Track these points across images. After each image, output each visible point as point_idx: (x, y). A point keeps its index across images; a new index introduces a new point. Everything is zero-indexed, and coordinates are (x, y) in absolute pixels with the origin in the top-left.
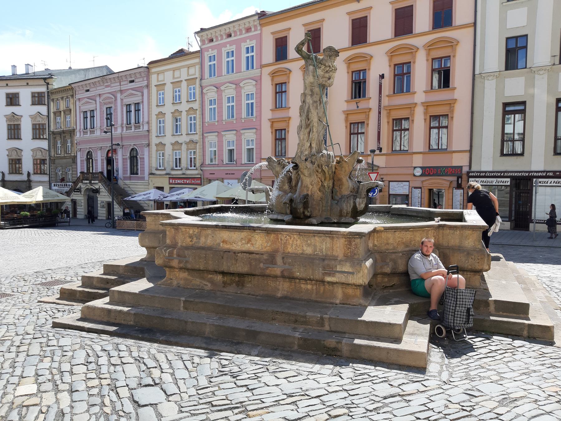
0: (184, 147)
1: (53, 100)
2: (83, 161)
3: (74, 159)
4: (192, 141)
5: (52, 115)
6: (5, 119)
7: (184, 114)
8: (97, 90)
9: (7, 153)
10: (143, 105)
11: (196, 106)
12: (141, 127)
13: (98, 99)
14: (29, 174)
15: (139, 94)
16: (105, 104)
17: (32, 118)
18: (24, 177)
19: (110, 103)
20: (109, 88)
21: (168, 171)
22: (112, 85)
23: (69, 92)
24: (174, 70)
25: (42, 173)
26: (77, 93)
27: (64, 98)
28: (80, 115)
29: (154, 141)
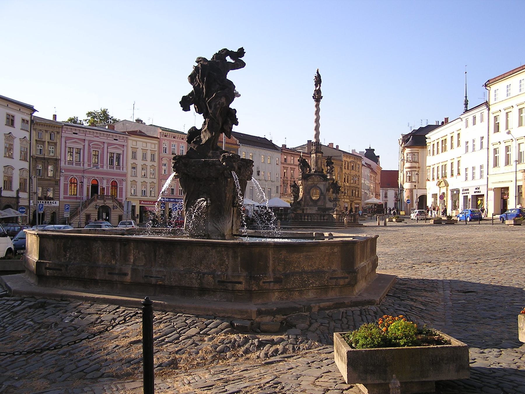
1: (35, 129)
2: (68, 184)
3: (57, 183)
5: (33, 142)
6: (4, 137)
7: (149, 167)
8: (85, 136)
10: (123, 156)
11: (156, 164)
14: (18, 192)
15: (123, 149)
18: (13, 194)
19: (97, 148)
22: (101, 137)
23: (55, 128)
25: (25, 191)
26: (63, 132)
27: (49, 132)
29: (130, 179)
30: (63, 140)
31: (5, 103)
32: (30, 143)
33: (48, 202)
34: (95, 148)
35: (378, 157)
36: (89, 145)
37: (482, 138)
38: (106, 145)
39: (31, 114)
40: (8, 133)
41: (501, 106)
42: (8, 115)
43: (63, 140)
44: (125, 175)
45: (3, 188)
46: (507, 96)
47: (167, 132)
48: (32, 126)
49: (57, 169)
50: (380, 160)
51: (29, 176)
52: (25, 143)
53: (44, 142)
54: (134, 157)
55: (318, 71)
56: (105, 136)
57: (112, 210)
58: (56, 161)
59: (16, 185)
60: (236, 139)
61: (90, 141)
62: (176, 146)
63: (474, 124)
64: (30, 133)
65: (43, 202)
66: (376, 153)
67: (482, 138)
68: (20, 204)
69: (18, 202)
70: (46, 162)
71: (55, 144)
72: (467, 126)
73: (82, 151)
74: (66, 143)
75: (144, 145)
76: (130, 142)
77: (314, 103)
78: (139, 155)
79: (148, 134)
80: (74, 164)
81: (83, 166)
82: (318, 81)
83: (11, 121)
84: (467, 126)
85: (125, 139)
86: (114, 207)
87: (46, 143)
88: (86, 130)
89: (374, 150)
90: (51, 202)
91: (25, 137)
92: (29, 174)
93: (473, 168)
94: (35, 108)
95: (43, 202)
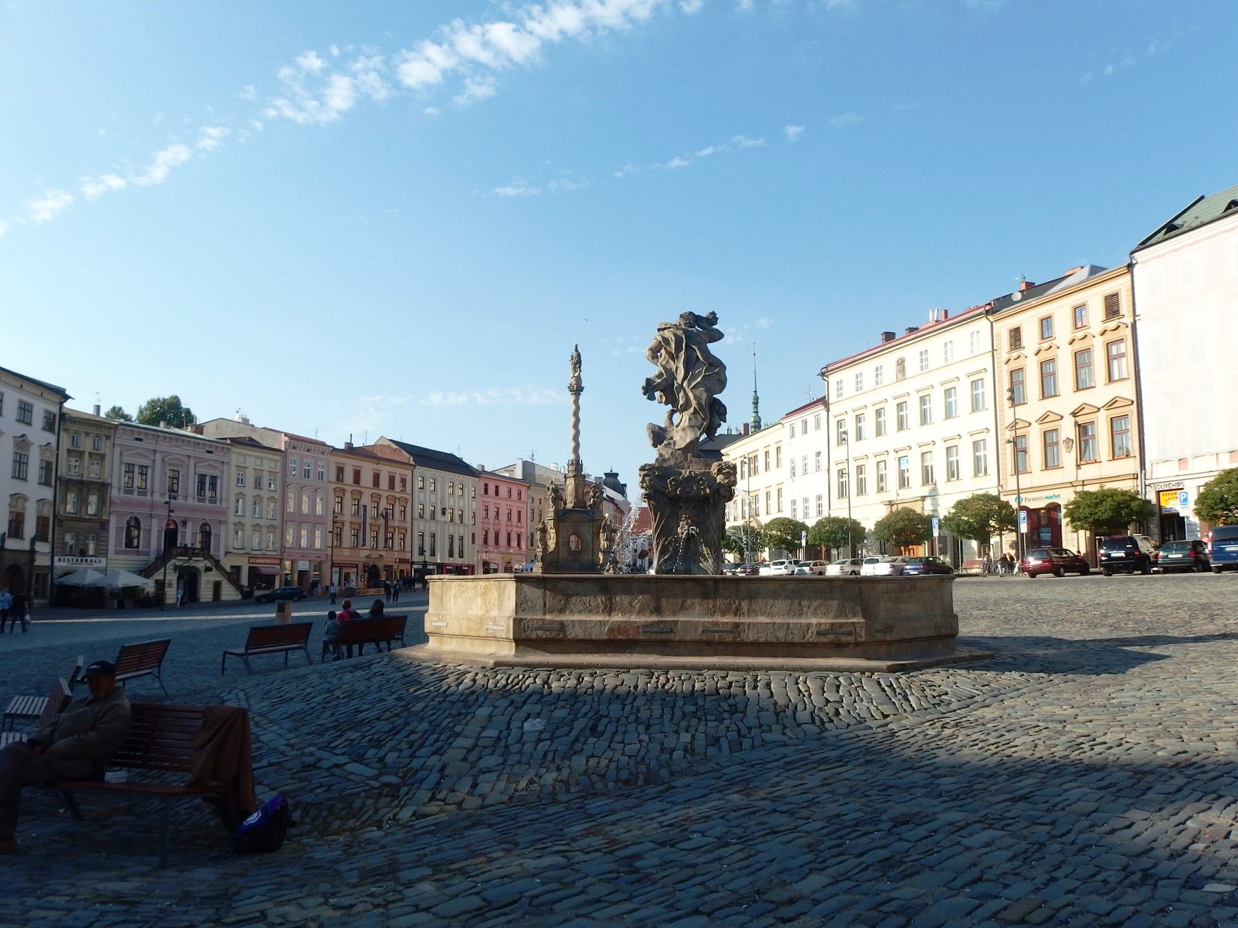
0: (264, 530)
1: (66, 430)
3: (104, 525)
4: (272, 526)
5: (63, 453)
7: (265, 500)
9: (8, 500)
11: (277, 495)
12: (218, 503)
13: (158, 457)
14: (33, 541)
16: (170, 465)
17: (41, 450)
18: (24, 545)
19: (178, 466)
20: (178, 449)
21: (248, 550)
22: (184, 447)
23: (103, 430)
24: (257, 457)
25: (45, 539)
26: (117, 435)
27: (91, 435)
28: (120, 467)
29: (232, 519)
30: (117, 450)
31: (18, 383)
32: (58, 455)
33: (86, 560)
34: (174, 465)
35: (625, 485)
36: (163, 460)
37: (818, 454)
38: (192, 462)
39: (61, 404)
40: (19, 435)
41: (849, 406)
42: (21, 402)
43: (117, 450)
44: (224, 512)
45: (7, 535)
46: (857, 390)
47: (296, 442)
48: (62, 424)
49: (102, 502)
50: (628, 490)
51: (52, 512)
52: (48, 454)
53: (81, 453)
54: (240, 481)
55: (576, 347)
56: (192, 444)
57: (203, 573)
58: (102, 488)
59: (30, 529)
60: (408, 455)
61: (165, 454)
62: (312, 465)
63: (805, 431)
64: (56, 437)
65: (77, 560)
66: (621, 479)
67: (818, 454)
68: (36, 563)
69: (33, 560)
70: (85, 489)
71: (102, 456)
72: (793, 435)
73: (150, 471)
74: (121, 454)
75: (259, 462)
76: (234, 456)
77: (572, 398)
78: (250, 479)
79: (264, 443)
80: (135, 493)
81: (152, 495)
82: (577, 363)
83: (25, 411)
84: (793, 435)
85: (226, 450)
86: (208, 569)
87: (86, 456)
88: (159, 434)
89: (617, 474)
90: (91, 561)
91: (49, 443)
92: (52, 509)
93: (806, 500)
94: (67, 392)
95: (77, 560)
